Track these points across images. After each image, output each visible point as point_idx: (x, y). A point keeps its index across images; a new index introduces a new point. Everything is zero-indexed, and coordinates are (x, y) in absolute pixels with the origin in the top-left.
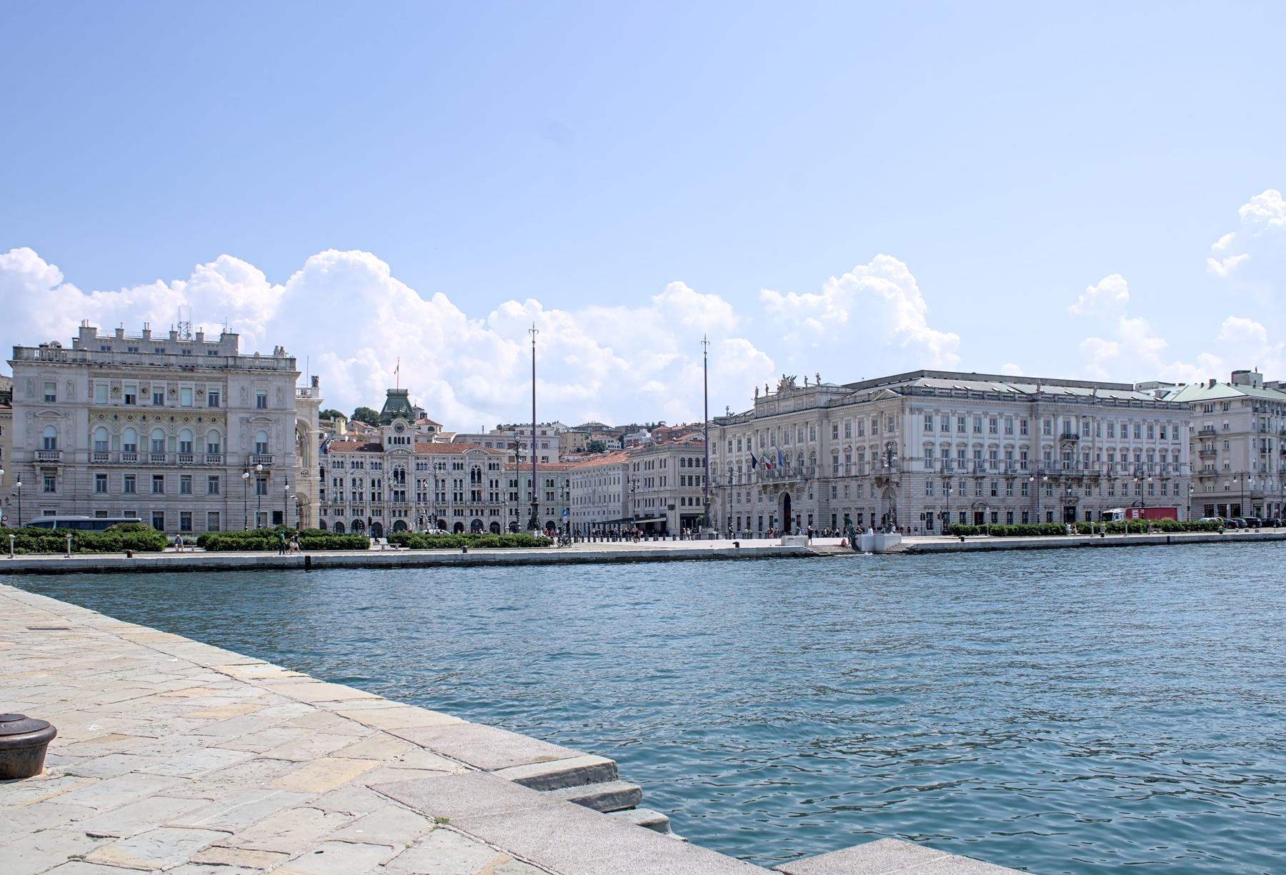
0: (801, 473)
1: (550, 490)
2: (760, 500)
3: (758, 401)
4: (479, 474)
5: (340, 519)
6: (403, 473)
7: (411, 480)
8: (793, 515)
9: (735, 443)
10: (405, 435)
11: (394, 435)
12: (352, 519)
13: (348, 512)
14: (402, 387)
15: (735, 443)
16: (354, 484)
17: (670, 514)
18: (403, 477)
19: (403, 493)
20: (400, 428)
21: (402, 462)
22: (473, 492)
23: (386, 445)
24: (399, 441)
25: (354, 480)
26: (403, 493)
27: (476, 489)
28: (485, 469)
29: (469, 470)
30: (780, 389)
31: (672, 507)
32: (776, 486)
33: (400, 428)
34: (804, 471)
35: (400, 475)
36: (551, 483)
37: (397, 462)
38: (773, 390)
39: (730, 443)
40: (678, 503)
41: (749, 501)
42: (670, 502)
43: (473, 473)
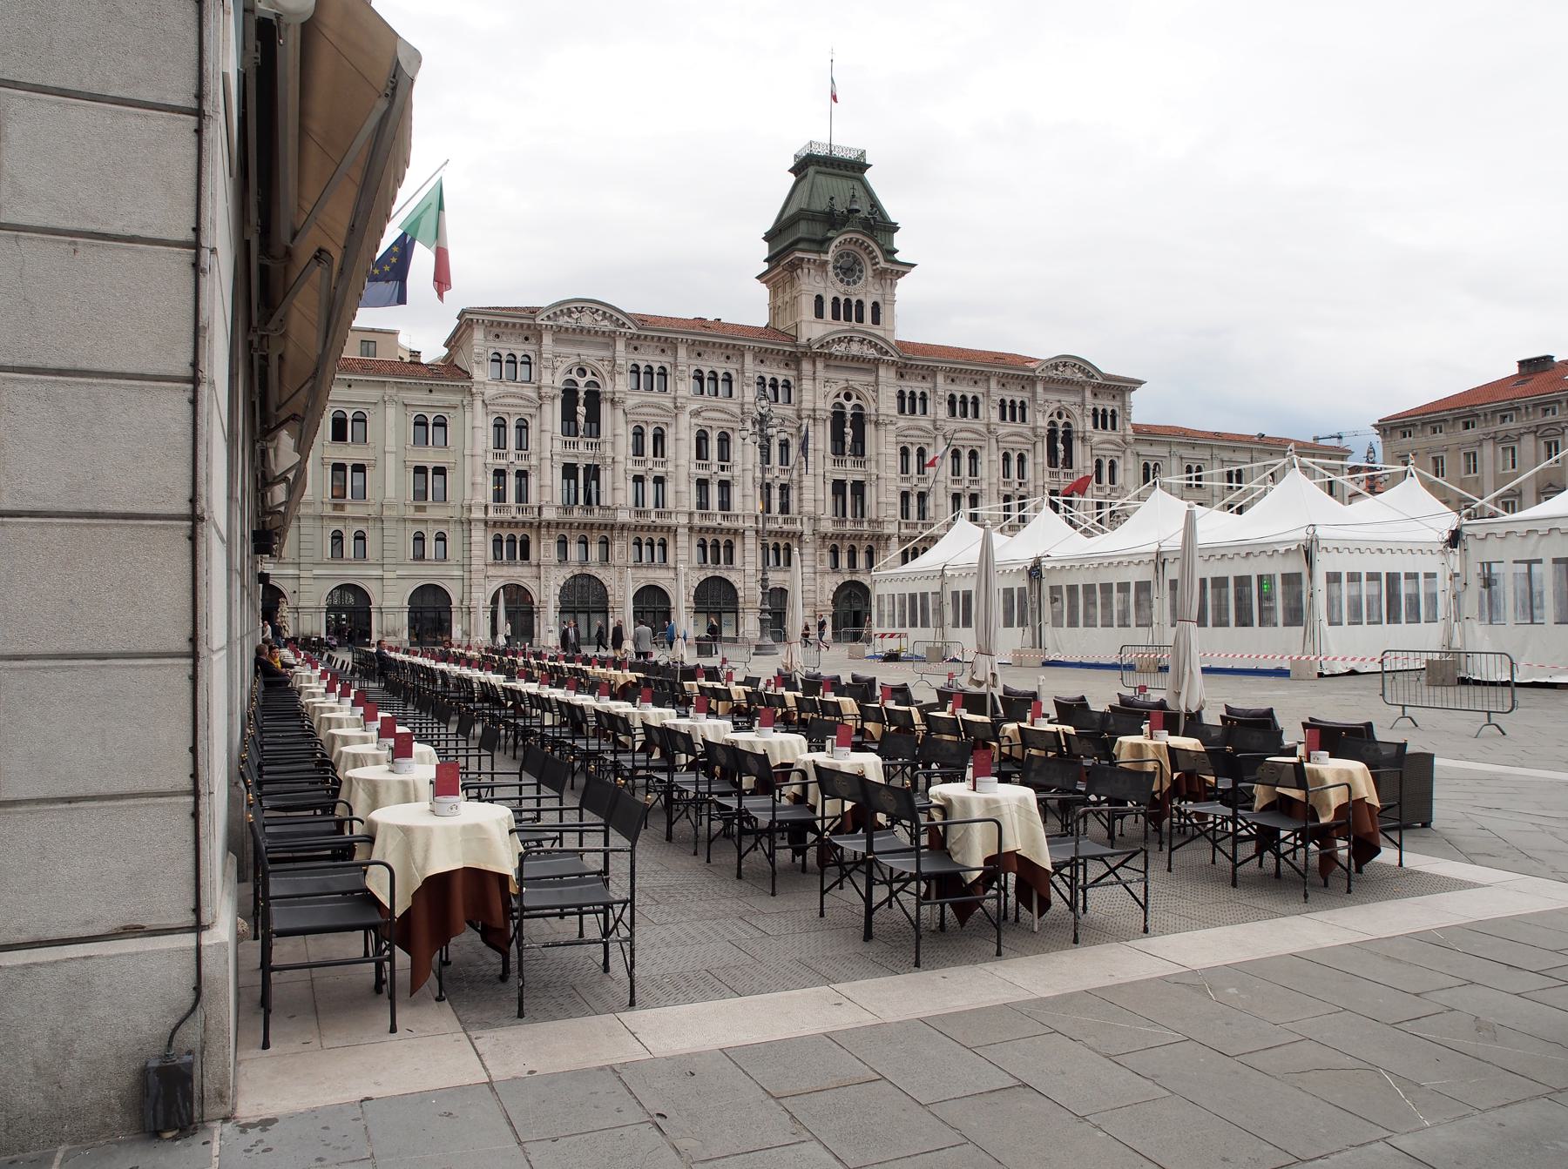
5: (661, 577)
6: (859, 420)
7: (883, 445)
10: (865, 291)
11: (832, 289)
12: (697, 577)
13: (685, 552)
16: (701, 453)
19: (859, 487)
20: (848, 270)
21: (858, 380)
25: (702, 438)
28: (1083, 425)
33: (848, 270)
35: (849, 430)
37: (841, 380)
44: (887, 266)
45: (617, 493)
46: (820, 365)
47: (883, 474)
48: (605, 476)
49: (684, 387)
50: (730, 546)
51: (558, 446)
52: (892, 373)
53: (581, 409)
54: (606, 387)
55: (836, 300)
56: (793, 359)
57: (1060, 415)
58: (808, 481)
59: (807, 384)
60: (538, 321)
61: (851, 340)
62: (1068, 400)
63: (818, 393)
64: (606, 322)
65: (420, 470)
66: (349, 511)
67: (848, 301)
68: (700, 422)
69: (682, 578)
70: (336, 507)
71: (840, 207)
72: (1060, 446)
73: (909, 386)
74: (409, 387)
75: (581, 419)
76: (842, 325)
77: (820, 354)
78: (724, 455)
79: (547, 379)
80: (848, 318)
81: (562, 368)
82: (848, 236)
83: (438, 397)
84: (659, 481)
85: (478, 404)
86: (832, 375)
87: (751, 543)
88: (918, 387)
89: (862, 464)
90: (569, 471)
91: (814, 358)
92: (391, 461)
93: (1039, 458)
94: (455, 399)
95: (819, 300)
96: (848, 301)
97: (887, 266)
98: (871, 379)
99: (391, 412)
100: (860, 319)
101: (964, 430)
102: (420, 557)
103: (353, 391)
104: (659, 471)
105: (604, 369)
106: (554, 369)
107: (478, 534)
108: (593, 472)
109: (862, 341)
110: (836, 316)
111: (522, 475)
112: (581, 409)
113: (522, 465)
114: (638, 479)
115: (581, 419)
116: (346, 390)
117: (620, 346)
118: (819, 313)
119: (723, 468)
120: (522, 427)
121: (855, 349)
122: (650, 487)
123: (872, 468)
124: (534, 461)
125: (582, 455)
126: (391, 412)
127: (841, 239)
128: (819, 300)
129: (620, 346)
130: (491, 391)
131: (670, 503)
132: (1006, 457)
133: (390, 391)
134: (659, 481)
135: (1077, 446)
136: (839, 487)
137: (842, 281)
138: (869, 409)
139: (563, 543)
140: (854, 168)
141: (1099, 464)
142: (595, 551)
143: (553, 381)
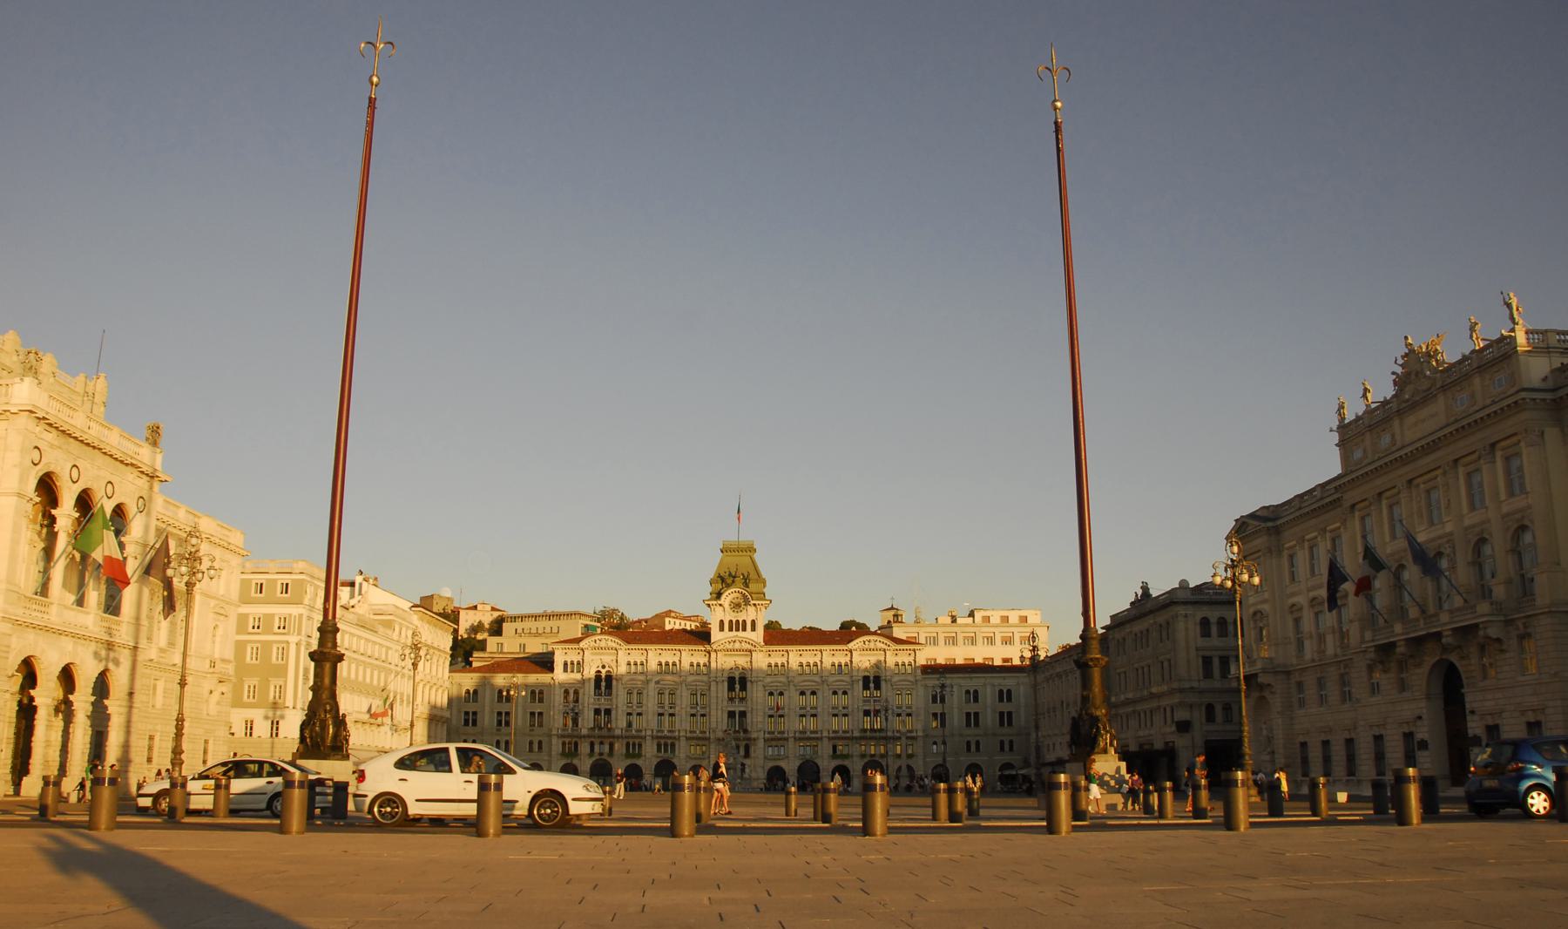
0: (1485, 593)
1: (1005, 707)
2: (1375, 689)
3: (1349, 434)
8: (1475, 727)
9: (1302, 557)
11: (729, 616)
14: (745, 538)
15: (1302, 557)
17: (1181, 742)
18: (743, 688)
19: (743, 714)
20: (736, 606)
23: (716, 635)
26: (743, 714)
30: (1401, 382)
31: (1184, 727)
32: (1418, 642)
34: (1499, 592)
36: (1005, 695)
38: (1383, 390)
39: (1291, 557)
40: (1198, 717)
41: (1346, 697)
42: (1182, 715)
45: (619, 722)
50: (673, 745)
58: (713, 713)
65: (532, 714)
69: (649, 757)
76: (734, 633)
87: (683, 742)
90: (597, 712)
95: (722, 622)
102: (531, 750)
107: (554, 741)
108: (608, 712)
110: (731, 629)
118: (722, 629)
121: (737, 645)
125: (603, 703)
128: (722, 622)
135: (883, 684)
136: (731, 714)
139: (592, 745)
140: (751, 549)
142: (606, 748)
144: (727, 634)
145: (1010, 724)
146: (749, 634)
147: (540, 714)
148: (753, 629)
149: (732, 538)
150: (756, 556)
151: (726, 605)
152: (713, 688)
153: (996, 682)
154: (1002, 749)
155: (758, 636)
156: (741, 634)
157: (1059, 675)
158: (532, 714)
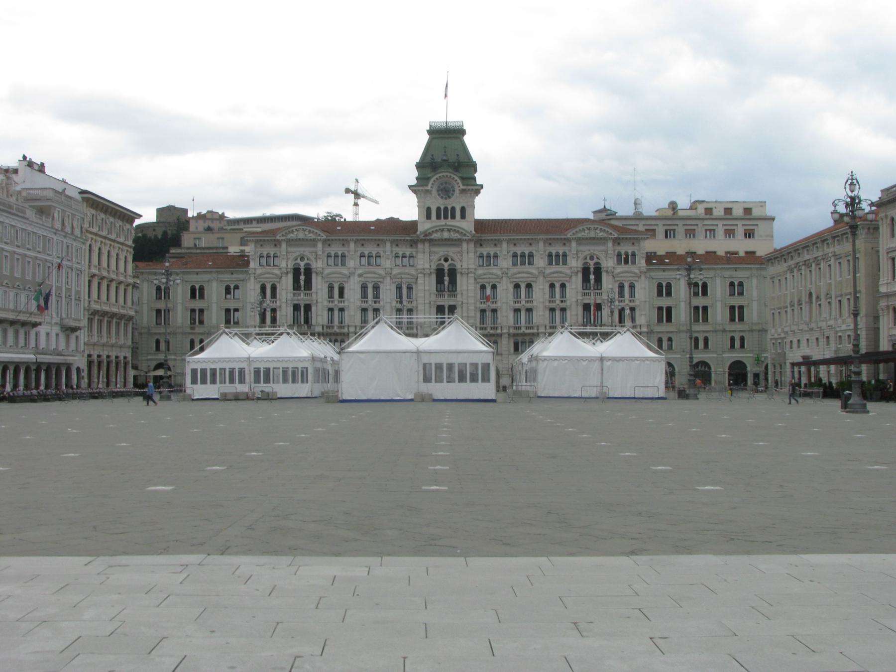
4: (598, 271)
6: (453, 273)
10: (456, 202)
11: (436, 202)
14: (453, 118)
16: (364, 295)
18: (453, 282)
21: (451, 251)
22: (586, 307)
24: (446, 213)
25: (364, 287)
27: (590, 300)
28: (608, 263)
29: (575, 263)
33: (446, 192)
37: (441, 251)
43: (586, 271)
44: (465, 187)
46: (427, 245)
47: (465, 301)
48: (313, 309)
49: (387, 263)
51: (290, 296)
52: (472, 245)
53: (302, 277)
54: (314, 265)
55: (438, 209)
56: (413, 243)
57: (592, 258)
59: (420, 256)
60: (278, 238)
61: (442, 230)
62: (596, 249)
63: (425, 260)
64: (311, 235)
66: (197, 330)
67: (446, 209)
68: (363, 279)
70: (192, 328)
71: (438, 159)
72: (592, 277)
73: (485, 250)
74: (222, 273)
75: (302, 283)
76: (442, 222)
77: (428, 239)
78: (376, 296)
79: (283, 265)
80: (446, 217)
81: (292, 257)
82: (441, 175)
83: (235, 276)
84: (341, 310)
85: (252, 278)
86: (434, 249)
88: (492, 250)
89: (455, 296)
90: (296, 308)
91: (423, 241)
92: (214, 308)
93: (575, 285)
94: (242, 276)
95: (429, 210)
96: (446, 209)
97: (465, 187)
98: (458, 249)
99: (214, 284)
100: (453, 217)
101: (524, 273)
103: (199, 276)
104: (341, 305)
105: (312, 257)
106: (288, 259)
108: (308, 308)
109: (449, 230)
110: (438, 217)
111: (274, 311)
112: (302, 277)
113: (273, 306)
114: (331, 310)
115: (302, 283)
116: (195, 276)
117: (320, 245)
119: (375, 302)
120: (274, 288)
121: (446, 235)
122: (336, 313)
123: (459, 297)
124: (278, 304)
125: (302, 298)
126: (214, 284)
127: (437, 176)
128: (429, 210)
129: (320, 245)
130: (259, 272)
131: (347, 321)
132: (552, 286)
133: (215, 275)
134: (341, 310)
135: (604, 277)
137: (442, 198)
138: (458, 266)
141: (621, 287)
143: (285, 264)
144: (434, 222)
145: (741, 319)
146: (457, 222)
147: (236, 310)
148: (463, 216)
149: (440, 118)
150: (466, 139)
151: (434, 192)
152: (420, 281)
153: (727, 274)
154: (732, 346)
155: (467, 226)
156: (450, 222)
157: (807, 264)
158: (228, 311)
